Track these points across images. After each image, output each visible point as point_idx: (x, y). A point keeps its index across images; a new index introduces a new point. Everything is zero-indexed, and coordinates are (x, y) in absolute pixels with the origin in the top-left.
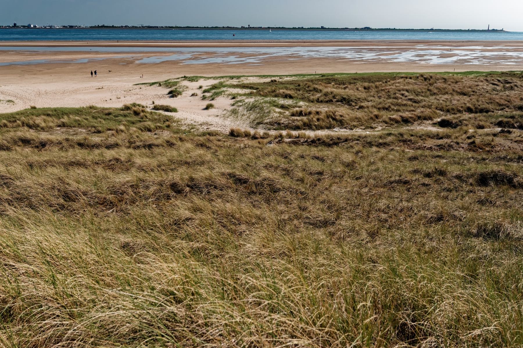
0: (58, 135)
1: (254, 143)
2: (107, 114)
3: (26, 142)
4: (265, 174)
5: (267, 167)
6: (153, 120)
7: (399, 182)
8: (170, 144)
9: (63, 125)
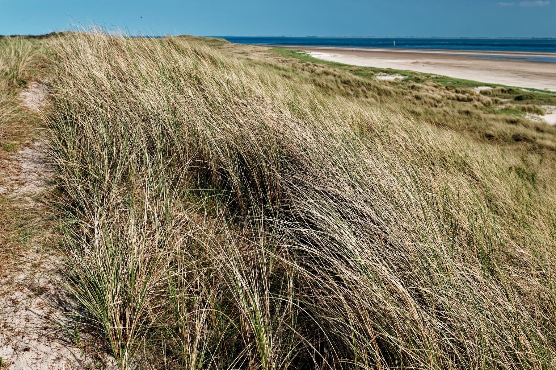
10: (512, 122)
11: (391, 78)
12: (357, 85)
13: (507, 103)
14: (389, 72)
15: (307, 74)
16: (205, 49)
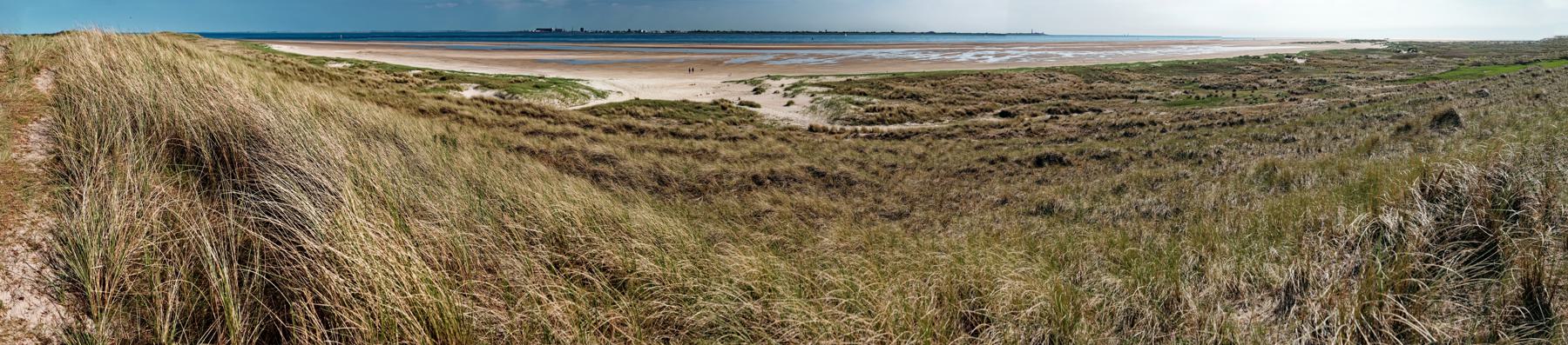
0: (654, 124)
1: (831, 138)
2: (697, 107)
3: (628, 128)
4: (842, 167)
5: (844, 161)
6: (739, 115)
7: (967, 171)
8: (753, 138)
9: (659, 115)
10: (440, 98)
11: (340, 65)
12: (312, 72)
13: (435, 83)
14: (338, 60)
15: (268, 63)
16: (182, 43)
